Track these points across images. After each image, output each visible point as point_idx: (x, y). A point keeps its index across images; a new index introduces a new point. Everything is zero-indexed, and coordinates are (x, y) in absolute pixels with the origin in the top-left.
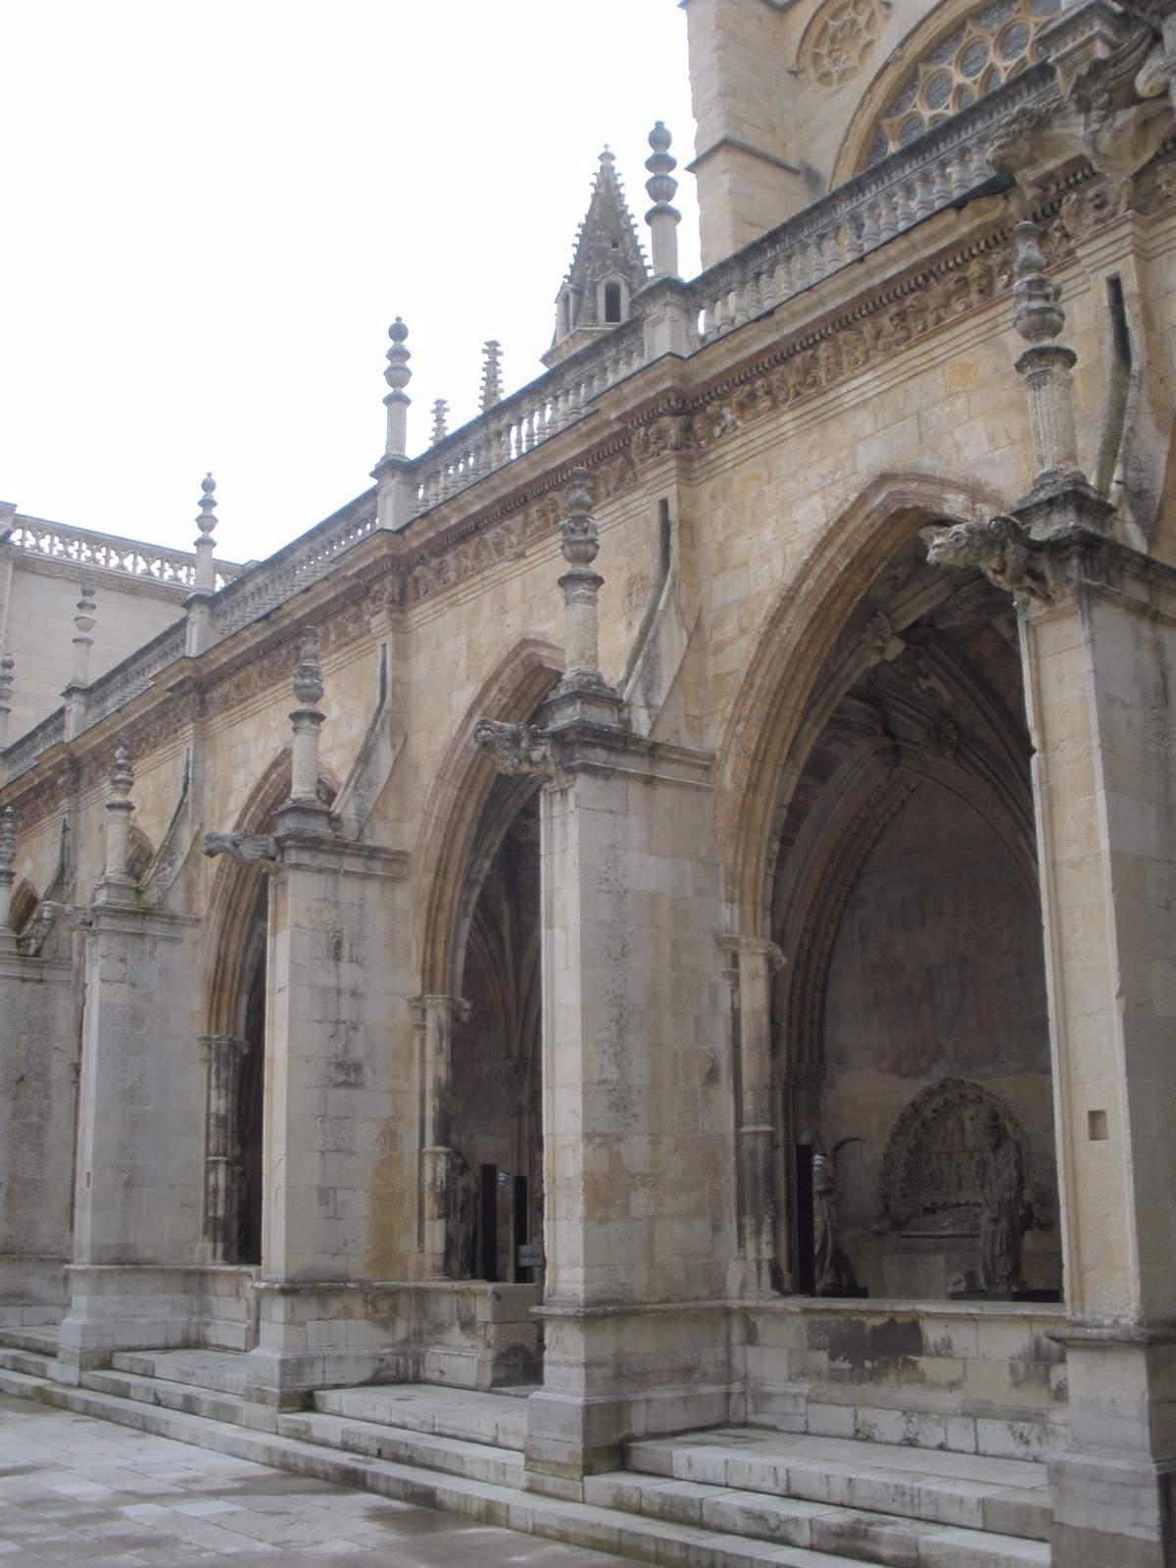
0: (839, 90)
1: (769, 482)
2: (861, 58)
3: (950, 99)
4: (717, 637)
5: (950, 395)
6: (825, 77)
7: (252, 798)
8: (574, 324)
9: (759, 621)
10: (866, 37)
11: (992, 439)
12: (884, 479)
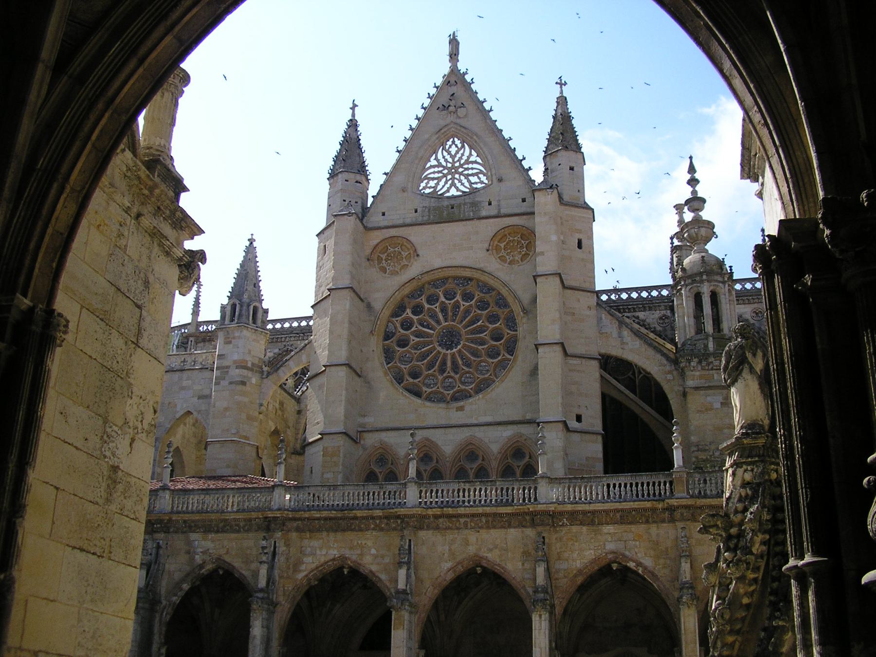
0: (389, 277)
1: (576, 542)
2: (401, 269)
3: (438, 305)
4: (556, 576)
5: (634, 540)
6: (384, 270)
7: (317, 568)
8: (238, 319)
9: (571, 575)
10: (405, 262)
11: (645, 554)
12: (613, 552)
